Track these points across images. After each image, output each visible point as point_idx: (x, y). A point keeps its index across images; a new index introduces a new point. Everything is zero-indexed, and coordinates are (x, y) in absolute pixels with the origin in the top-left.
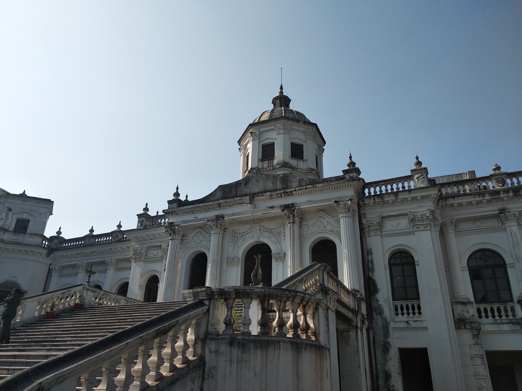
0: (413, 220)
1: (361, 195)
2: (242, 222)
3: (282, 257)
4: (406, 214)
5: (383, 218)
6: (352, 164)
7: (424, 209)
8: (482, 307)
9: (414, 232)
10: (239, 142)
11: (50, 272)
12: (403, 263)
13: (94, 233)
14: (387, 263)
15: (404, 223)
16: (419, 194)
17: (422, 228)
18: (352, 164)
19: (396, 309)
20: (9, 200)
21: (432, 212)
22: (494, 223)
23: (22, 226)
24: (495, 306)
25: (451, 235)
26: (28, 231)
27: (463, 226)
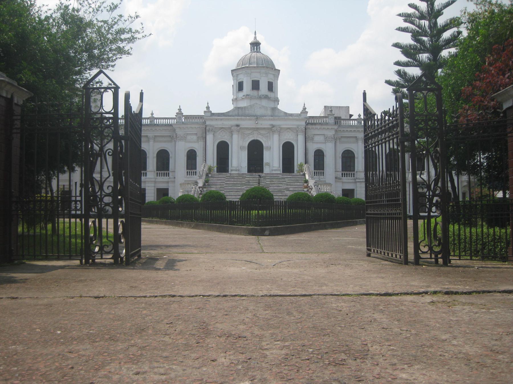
1: (307, 124)
2: (247, 129)
3: (269, 148)
6: (306, 109)
7: (331, 133)
8: (344, 172)
10: (232, 71)
12: (319, 155)
16: (330, 127)
18: (305, 109)
21: (334, 135)
22: (354, 139)
24: (348, 173)
25: (338, 144)
27: (343, 140)
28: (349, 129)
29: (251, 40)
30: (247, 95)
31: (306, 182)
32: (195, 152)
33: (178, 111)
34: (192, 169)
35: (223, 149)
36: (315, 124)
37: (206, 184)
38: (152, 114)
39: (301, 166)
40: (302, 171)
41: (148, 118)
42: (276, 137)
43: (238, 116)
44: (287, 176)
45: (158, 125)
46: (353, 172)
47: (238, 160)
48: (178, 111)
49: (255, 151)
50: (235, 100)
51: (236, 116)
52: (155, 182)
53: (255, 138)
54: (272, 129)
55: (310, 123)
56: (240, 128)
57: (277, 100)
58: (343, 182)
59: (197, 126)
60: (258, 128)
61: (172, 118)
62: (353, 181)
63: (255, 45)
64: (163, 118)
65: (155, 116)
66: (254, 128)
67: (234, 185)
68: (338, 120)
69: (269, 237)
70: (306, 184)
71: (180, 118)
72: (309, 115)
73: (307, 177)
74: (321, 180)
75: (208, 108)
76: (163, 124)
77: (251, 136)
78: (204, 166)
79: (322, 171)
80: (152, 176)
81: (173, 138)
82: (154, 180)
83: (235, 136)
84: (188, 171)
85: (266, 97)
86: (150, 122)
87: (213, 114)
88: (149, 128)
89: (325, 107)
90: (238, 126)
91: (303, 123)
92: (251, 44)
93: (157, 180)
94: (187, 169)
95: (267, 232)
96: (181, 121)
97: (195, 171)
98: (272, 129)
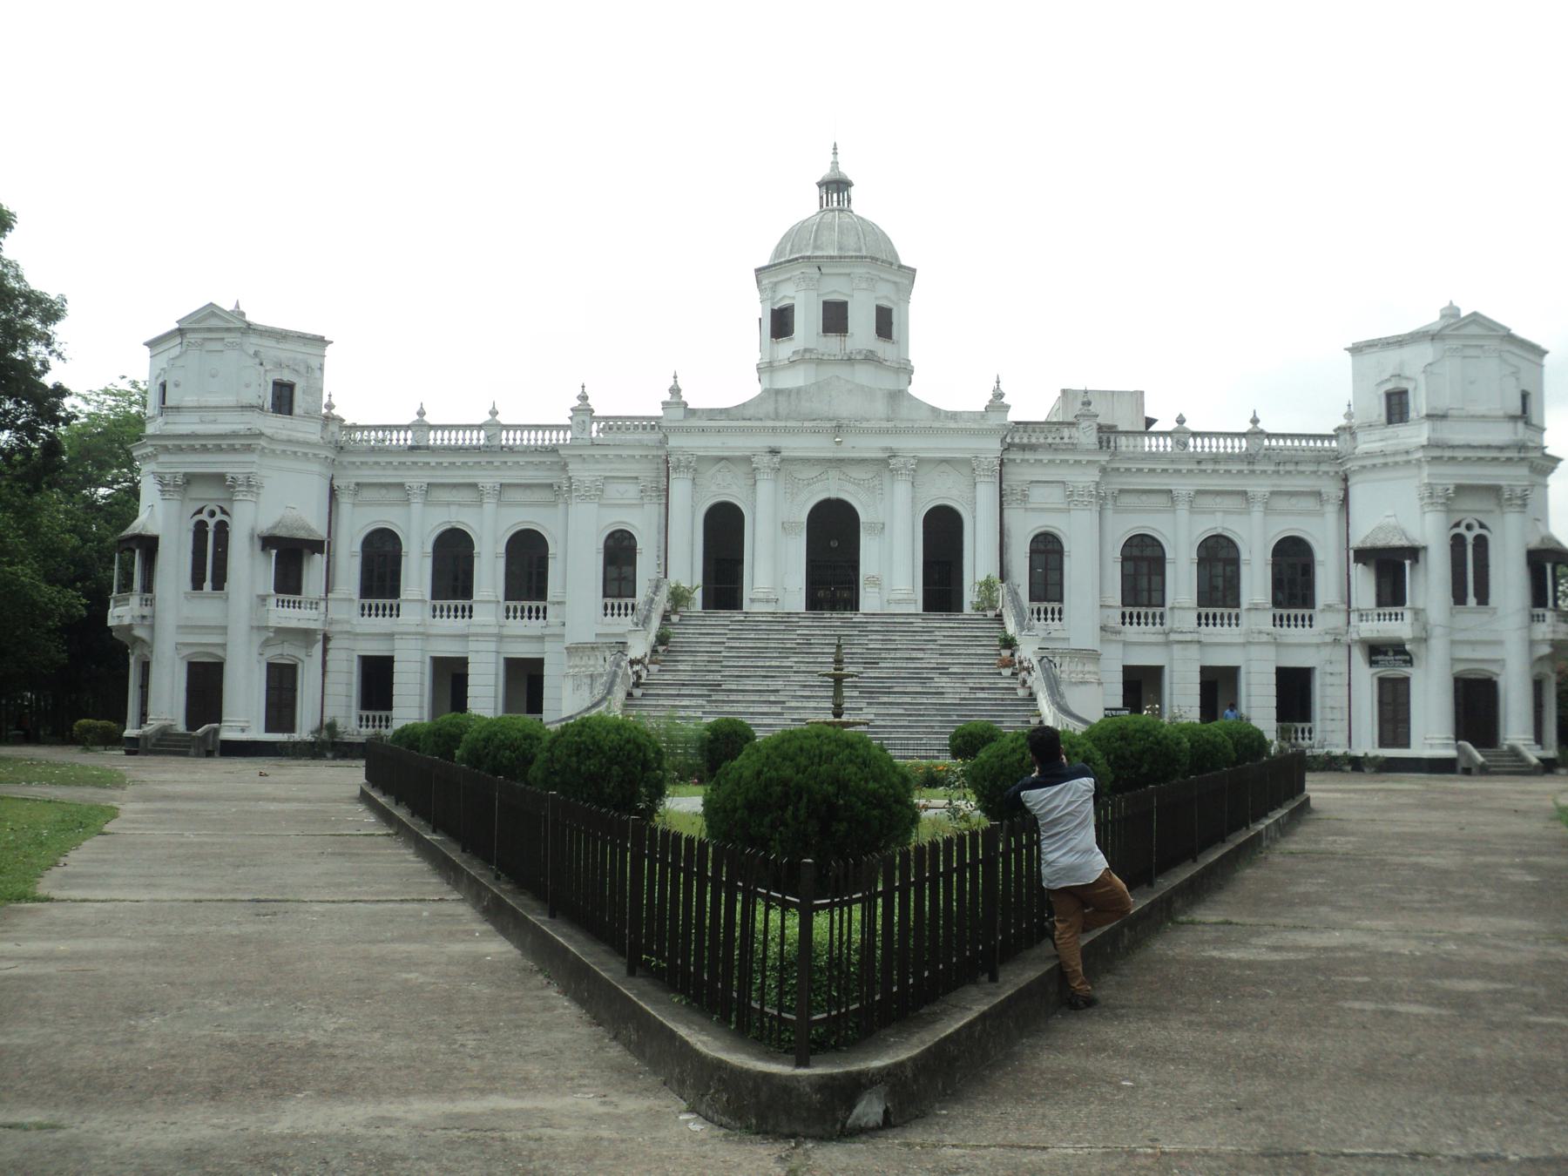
0: (1071, 495)
1: (1008, 448)
6: (1001, 395)
7: (1086, 478)
8: (1128, 610)
10: (759, 271)
11: (333, 494)
12: (1047, 550)
13: (430, 419)
18: (999, 395)
20: (254, 339)
22: (1162, 501)
23: (283, 398)
24: (1143, 610)
25: (1109, 513)
26: (296, 410)
27: (1126, 500)
28: (1146, 466)
29: (824, 171)
30: (806, 350)
31: (1009, 643)
32: (631, 536)
33: (577, 403)
34: (620, 596)
35: (724, 531)
36: (1032, 448)
37: (661, 649)
38: (494, 413)
39: (988, 585)
40: (993, 608)
41: (480, 427)
42: (901, 491)
43: (777, 417)
44: (938, 621)
45: (511, 449)
46: (1158, 610)
47: (776, 569)
48: (577, 403)
49: (833, 539)
50: (767, 368)
51: (768, 418)
52: (500, 638)
53: (833, 495)
54: (884, 464)
55: (1020, 442)
56: (783, 460)
57: (906, 370)
58: (1125, 644)
59: (638, 453)
60: (841, 460)
61: (558, 427)
62: (1161, 638)
63: (836, 186)
64: (529, 427)
65: (503, 419)
66: (830, 460)
67: (758, 653)
68: (1107, 433)
69: (891, 1144)
70: (1006, 653)
71: (584, 427)
72: (1013, 416)
73: (1011, 628)
74: (1054, 635)
75: (675, 391)
76: (528, 447)
77: (818, 486)
78: (657, 588)
79: (1056, 606)
80: (491, 620)
81: (557, 492)
82: (495, 630)
83: (765, 488)
84: (609, 601)
85: (870, 358)
86: (488, 438)
87: (693, 412)
88: (484, 459)
89: (1064, 392)
90: (774, 452)
91: (994, 446)
92: (820, 185)
93: (506, 631)
94: (605, 595)
95: (870, 1109)
96: (586, 436)
97: (629, 601)
98: (884, 464)
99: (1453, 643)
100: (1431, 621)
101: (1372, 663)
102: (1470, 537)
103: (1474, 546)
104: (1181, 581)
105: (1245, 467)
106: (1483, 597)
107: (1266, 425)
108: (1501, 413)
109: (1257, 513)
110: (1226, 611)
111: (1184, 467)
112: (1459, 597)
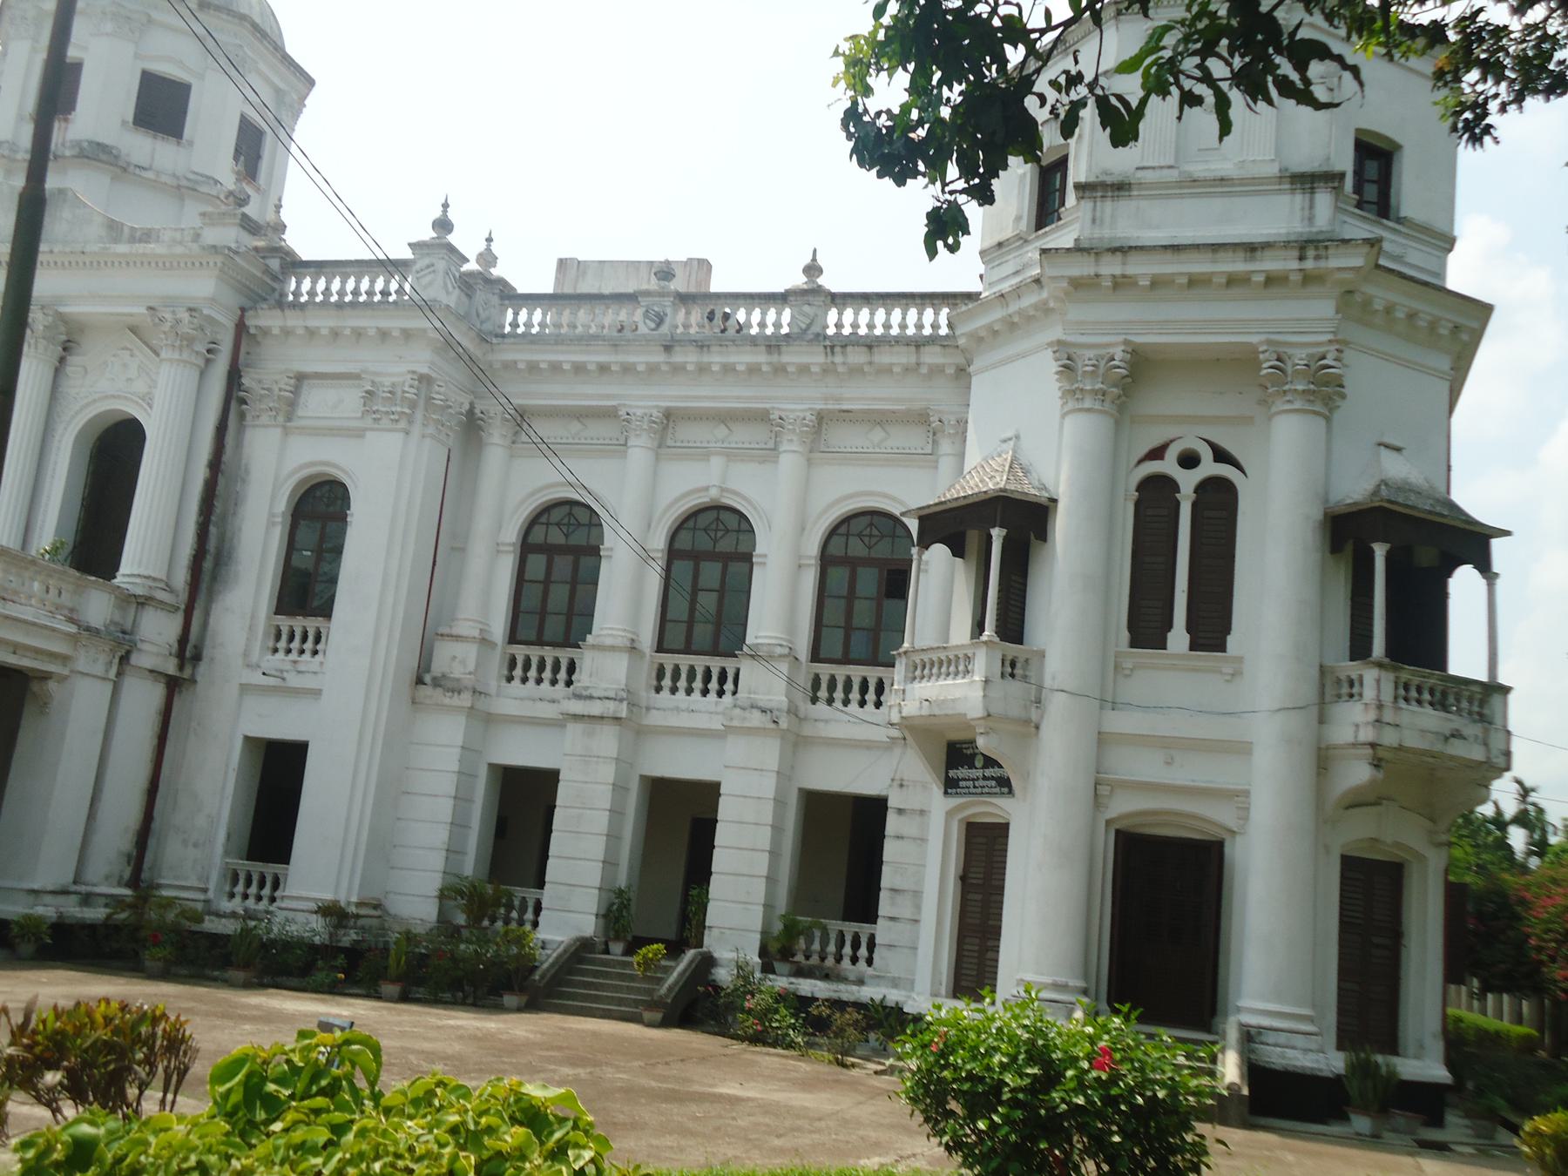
4: (357, 377)
5: (301, 378)
9: (365, 430)
14: (282, 505)
15: (347, 402)
17: (385, 423)
19: (278, 637)
21: (425, 379)
28: (567, 357)
74: (294, 681)
99: (1103, 740)
100: (1048, 683)
101: (950, 785)
102: (1188, 481)
103: (1195, 506)
104: (626, 596)
105: (761, 357)
106: (1211, 630)
107: (831, 281)
108: (1273, 170)
109: (790, 461)
110: (715, 664)
111: (640, 359)
112: (1147, 628)
